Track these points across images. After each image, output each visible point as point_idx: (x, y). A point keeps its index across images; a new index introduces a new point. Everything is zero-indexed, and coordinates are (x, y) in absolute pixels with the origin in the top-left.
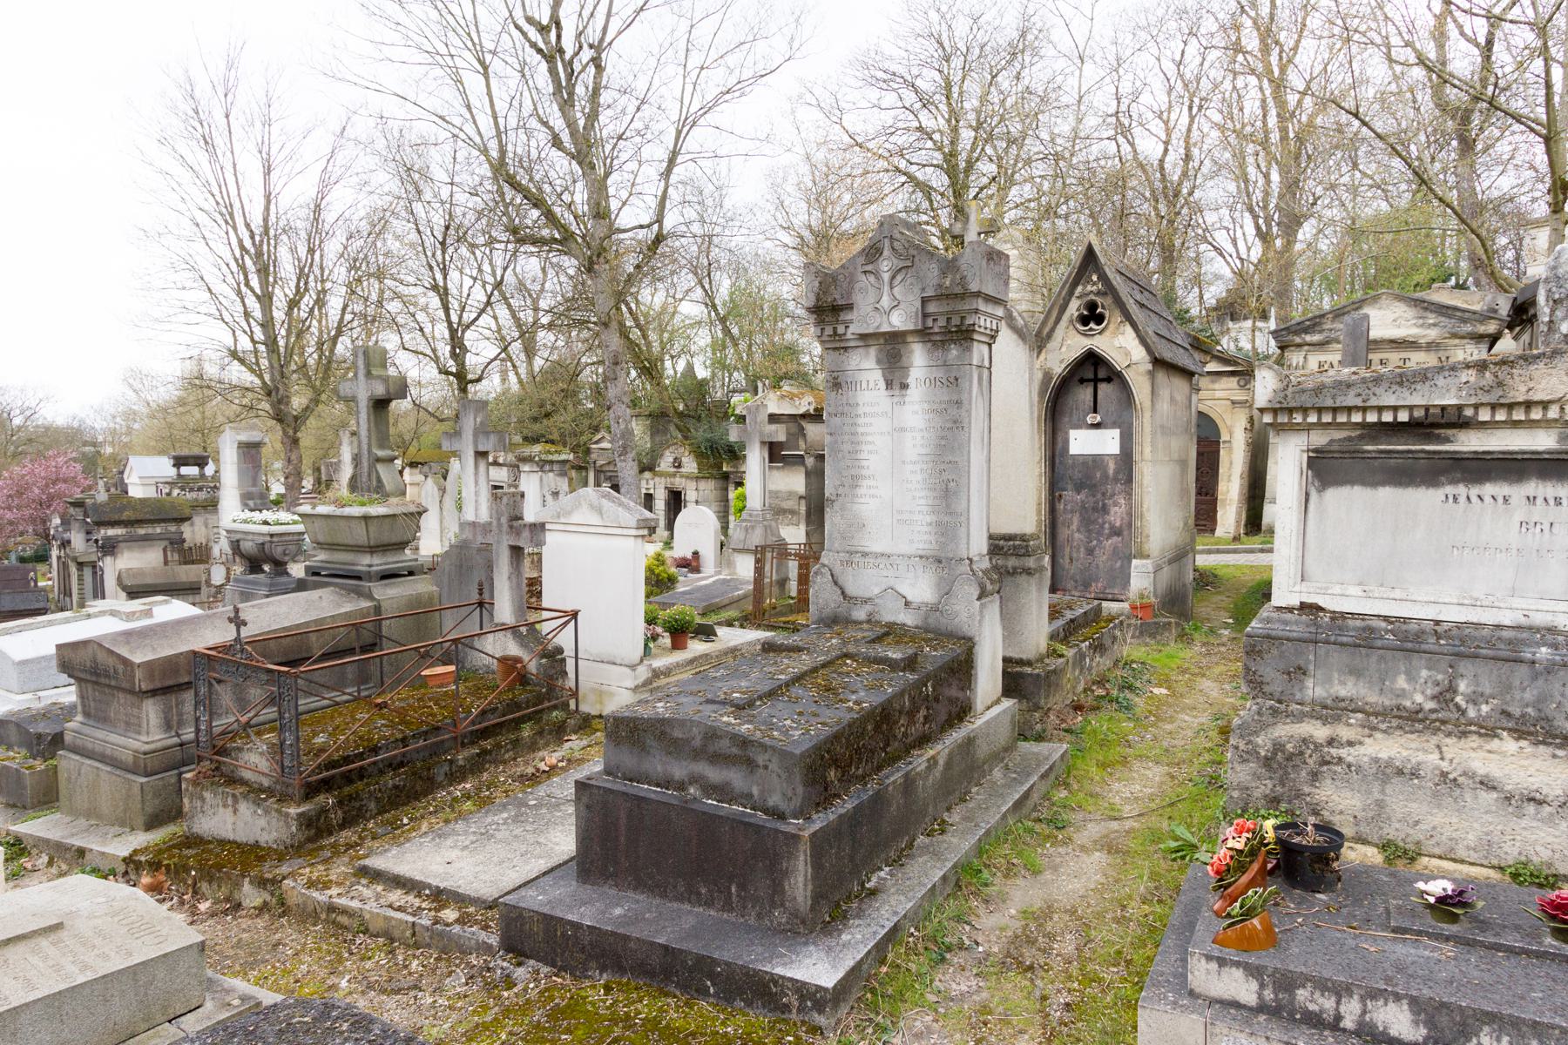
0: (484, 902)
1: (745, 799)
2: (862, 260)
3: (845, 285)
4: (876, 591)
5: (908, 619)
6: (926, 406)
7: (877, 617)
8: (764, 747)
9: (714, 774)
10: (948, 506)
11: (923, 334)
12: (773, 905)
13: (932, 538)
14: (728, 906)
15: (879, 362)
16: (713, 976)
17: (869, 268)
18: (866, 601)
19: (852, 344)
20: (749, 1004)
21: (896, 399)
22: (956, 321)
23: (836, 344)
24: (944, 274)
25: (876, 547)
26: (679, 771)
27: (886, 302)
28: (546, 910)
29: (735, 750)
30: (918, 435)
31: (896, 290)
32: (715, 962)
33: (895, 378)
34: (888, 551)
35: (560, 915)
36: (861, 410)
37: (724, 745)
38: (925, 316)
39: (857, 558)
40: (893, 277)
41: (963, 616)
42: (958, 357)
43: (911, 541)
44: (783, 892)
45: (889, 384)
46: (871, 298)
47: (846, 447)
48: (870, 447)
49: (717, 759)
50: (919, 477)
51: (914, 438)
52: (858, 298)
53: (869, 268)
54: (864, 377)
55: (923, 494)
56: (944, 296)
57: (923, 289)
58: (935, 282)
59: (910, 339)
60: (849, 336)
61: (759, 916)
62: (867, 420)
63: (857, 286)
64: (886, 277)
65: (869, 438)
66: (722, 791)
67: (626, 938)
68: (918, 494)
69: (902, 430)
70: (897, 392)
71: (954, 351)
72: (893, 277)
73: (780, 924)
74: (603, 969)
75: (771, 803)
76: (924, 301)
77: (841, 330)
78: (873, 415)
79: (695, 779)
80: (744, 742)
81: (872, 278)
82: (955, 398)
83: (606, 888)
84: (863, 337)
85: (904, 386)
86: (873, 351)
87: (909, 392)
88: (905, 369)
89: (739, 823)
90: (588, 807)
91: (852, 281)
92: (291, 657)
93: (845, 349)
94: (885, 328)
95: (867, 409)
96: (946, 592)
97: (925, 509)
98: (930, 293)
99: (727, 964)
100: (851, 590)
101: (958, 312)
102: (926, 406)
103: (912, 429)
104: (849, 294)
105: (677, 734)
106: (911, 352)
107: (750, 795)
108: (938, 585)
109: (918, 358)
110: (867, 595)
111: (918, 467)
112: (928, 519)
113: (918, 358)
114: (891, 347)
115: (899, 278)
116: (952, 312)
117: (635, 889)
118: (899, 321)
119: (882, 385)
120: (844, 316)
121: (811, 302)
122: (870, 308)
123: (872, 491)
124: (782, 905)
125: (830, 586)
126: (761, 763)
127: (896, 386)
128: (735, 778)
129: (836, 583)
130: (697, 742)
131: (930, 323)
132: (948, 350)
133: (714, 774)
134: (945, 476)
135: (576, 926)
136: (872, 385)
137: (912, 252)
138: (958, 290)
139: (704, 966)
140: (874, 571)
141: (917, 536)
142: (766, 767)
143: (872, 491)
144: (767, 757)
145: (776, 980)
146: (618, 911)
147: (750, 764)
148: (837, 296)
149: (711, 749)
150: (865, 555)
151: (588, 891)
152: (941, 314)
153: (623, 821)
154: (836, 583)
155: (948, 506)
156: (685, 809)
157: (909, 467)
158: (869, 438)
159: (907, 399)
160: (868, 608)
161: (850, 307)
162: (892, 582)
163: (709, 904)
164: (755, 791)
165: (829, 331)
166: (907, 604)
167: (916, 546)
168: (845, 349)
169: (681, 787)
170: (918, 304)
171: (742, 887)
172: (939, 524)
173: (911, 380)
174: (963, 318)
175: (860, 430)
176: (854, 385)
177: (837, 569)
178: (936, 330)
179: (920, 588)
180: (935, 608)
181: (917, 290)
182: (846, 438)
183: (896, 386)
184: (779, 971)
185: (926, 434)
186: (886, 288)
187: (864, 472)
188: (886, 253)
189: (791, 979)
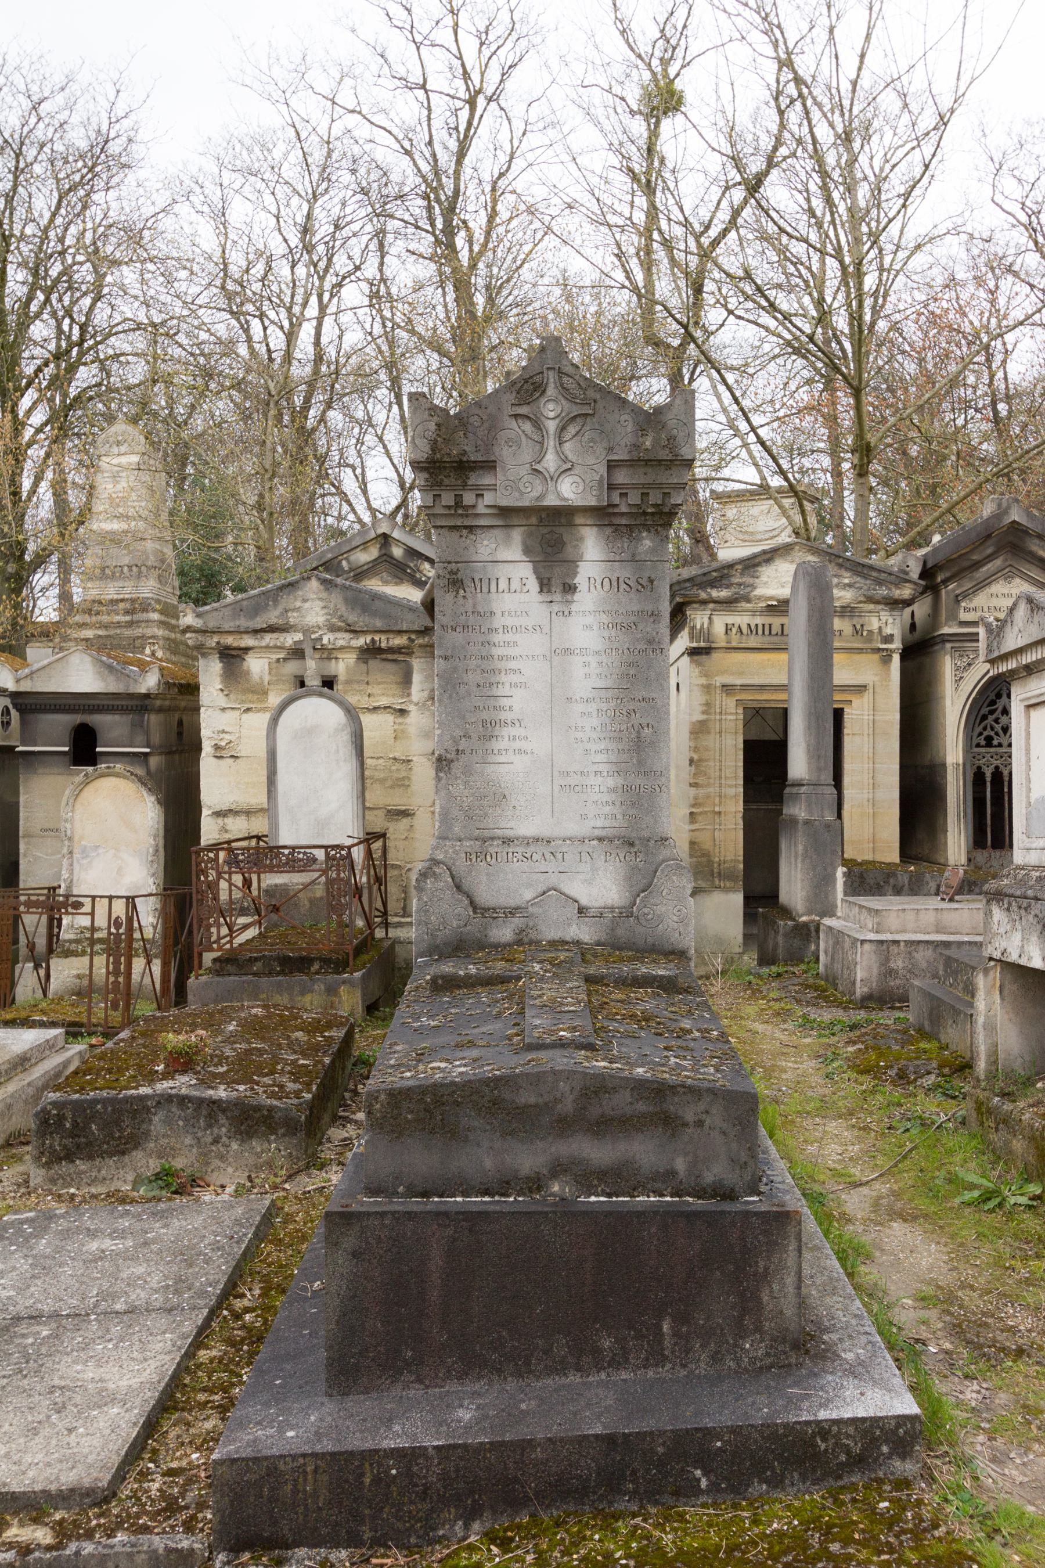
0: (90, 1492)
1: (663, 1179)
2: (510, 397)
3: (481, 432)
4: (528, 895)
5: (584, 932)
6: (605, 619)
7: (533, 935)
8: (694, 1092)
9: (598, 1152)
10: (641, 763)
11: (602, 515)
12: (741, 1333)
13: (617, 811)
14: (656, 1357)
15: (527, 551)
16: (705, 1460)
17: (524, 410)
18: (512, 912)
19: (483, 522)
20: (776, 1483)
21: (556, 607)
22: (655, 498)
23: (456, 519)
24: (642, 430)
25: (526, 829)
26: (528, 1158)
27: (550, 462)
28: (327, 1446)
29: (642, 1107)
30: (593, 661)
31: (567, 446)
32: (709, 1433)
33: (554, 573)
34: (545, 832)
35: (368, 1445)
36: (498, 622)
37: (622, 1102)
38: (611, 487)
39: (494, 847)
40: (563, 429)
41: (671, 921)
42: (653, 550)
43: (584, 817)
44: (759, 1305)
45: (544, 585)
46: (527, 454)
47: (472, 678)
48: (514, 678)
49: (603, 1127)
50: (595, 722)
51: (586, 664)
52: (504, 453)
53: (524, 410)
54: (503, 572)
55: (602, 746)
56: (641, 461)
57: (610, 449)
58: (629, 440)
59: (579, 520)
60: (481, 509)
61: (716, 1358)
62: (509, 637)
63: (503, 435)
64: (552, 426)
65: (513, 664)
66: (618, 1178)
67: (526, 1445)
68: (593, 747)
69: (568, 652)
70: (558, 597)
71: (647, 542)
72: (563, 429)
73: (753, 1361)
74: (470, 1516)
75: (709, 1178)
76: (612, 466)
77: (469, 498)
78: (517, 629)
79: (558, 1169)
80: (657, 1091)
81: (527, 427)
82: (650, 608)
83: (397, 1390)
84: (505, 512)
85: (570, 589)
86: (517, 536)
87: (577, 597)
88: (571, 565)
89: (666, 1216)
90: (355, 1254)
91: (494, 426)
92: (641, 886)
93: (471, 529)
94: (551, 501)
95: (509, 621)
96: (643, 884)
97: (604, 768)
98: (621, 455)
99: (734, 1430)
100: (486, 896)
101: (659, 486)
102: (605, 619)
103: (583, 652)
104: (489, 445)
105: (527, 1097)
106: (581, 539)
107: (672, 1173)
108: (629, 878)
109: (592, 551)
110: (512, 903)
111: (592, 708)
112: (611, 782)
113: (592, 551)
114: (549, 534)
115: (572, 430)
116: (650, 486)
117: (462, 1376)
118: (569, 491)
119: (533, 584)
120: (473, 479)
121: (423, 453)
122: (524, 470)
123: (518, 744)
124: (758, 1329)
125: (449, 894)
126: (690, 1117)
127: (557, 586)
128: (644, 1151)
129: (458, 887)
130: (568, 1106)
131: (616, 499)
132: (639, 539)
133: (598, 1152)
134: (636, 720)
135: (408, 1456)
136: (515, 584)
137: (591, 394)
138: (664, 455)
139: (691, 1447)
140: (525, 865)
141: (595, 807)
142: (700, 1124)
143: (518, 744)
144: (701, 1107)
145: (823, 1429)
146: (465, 1415)
147: (669, 1123)
148: (468, 447)
149: (594, 1112)
150: (507, 841)
151: (351, 1402)
152: (634, 486)
153: (437, 1261)
154: (458, 887)
155: (641, 763)
156: (568, 1213)
157: (579, 708)
158: (513, 664)
159: (574, 607)
160: (517, 922)
161: (490, 466)
162: (553, 880)
163: (618, 1362)
164: (680, 1165)
165: (448, 499)
166: (582, 911)
167: (592, 823)
168: (471, 529)
169: (535, 1184)
170: (603, 470)
171: (682, 1319)
172: (626, 789)
173: (581, 580)
174: (666, 495)
175: (497, 652)
176: (485, 584)
177: (461, 865)
178: (624, 509)
179: (601, 886)
180: (626, 912)
181: (600, 449)
182: (473, 663)
183: (557, 586)
184: (823, 1415)
185: (605, 659)
186: (551, 443)
187: (504, 716)
188: (551, 391)
189: (854, 1421)
